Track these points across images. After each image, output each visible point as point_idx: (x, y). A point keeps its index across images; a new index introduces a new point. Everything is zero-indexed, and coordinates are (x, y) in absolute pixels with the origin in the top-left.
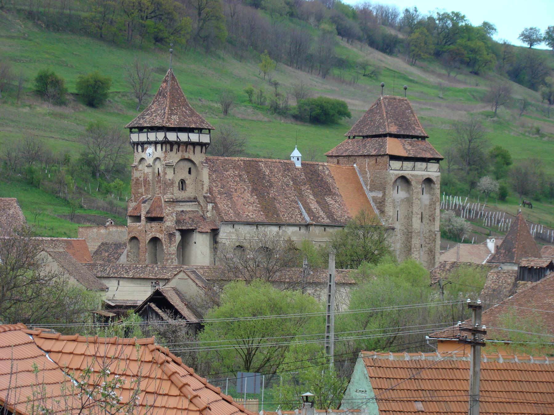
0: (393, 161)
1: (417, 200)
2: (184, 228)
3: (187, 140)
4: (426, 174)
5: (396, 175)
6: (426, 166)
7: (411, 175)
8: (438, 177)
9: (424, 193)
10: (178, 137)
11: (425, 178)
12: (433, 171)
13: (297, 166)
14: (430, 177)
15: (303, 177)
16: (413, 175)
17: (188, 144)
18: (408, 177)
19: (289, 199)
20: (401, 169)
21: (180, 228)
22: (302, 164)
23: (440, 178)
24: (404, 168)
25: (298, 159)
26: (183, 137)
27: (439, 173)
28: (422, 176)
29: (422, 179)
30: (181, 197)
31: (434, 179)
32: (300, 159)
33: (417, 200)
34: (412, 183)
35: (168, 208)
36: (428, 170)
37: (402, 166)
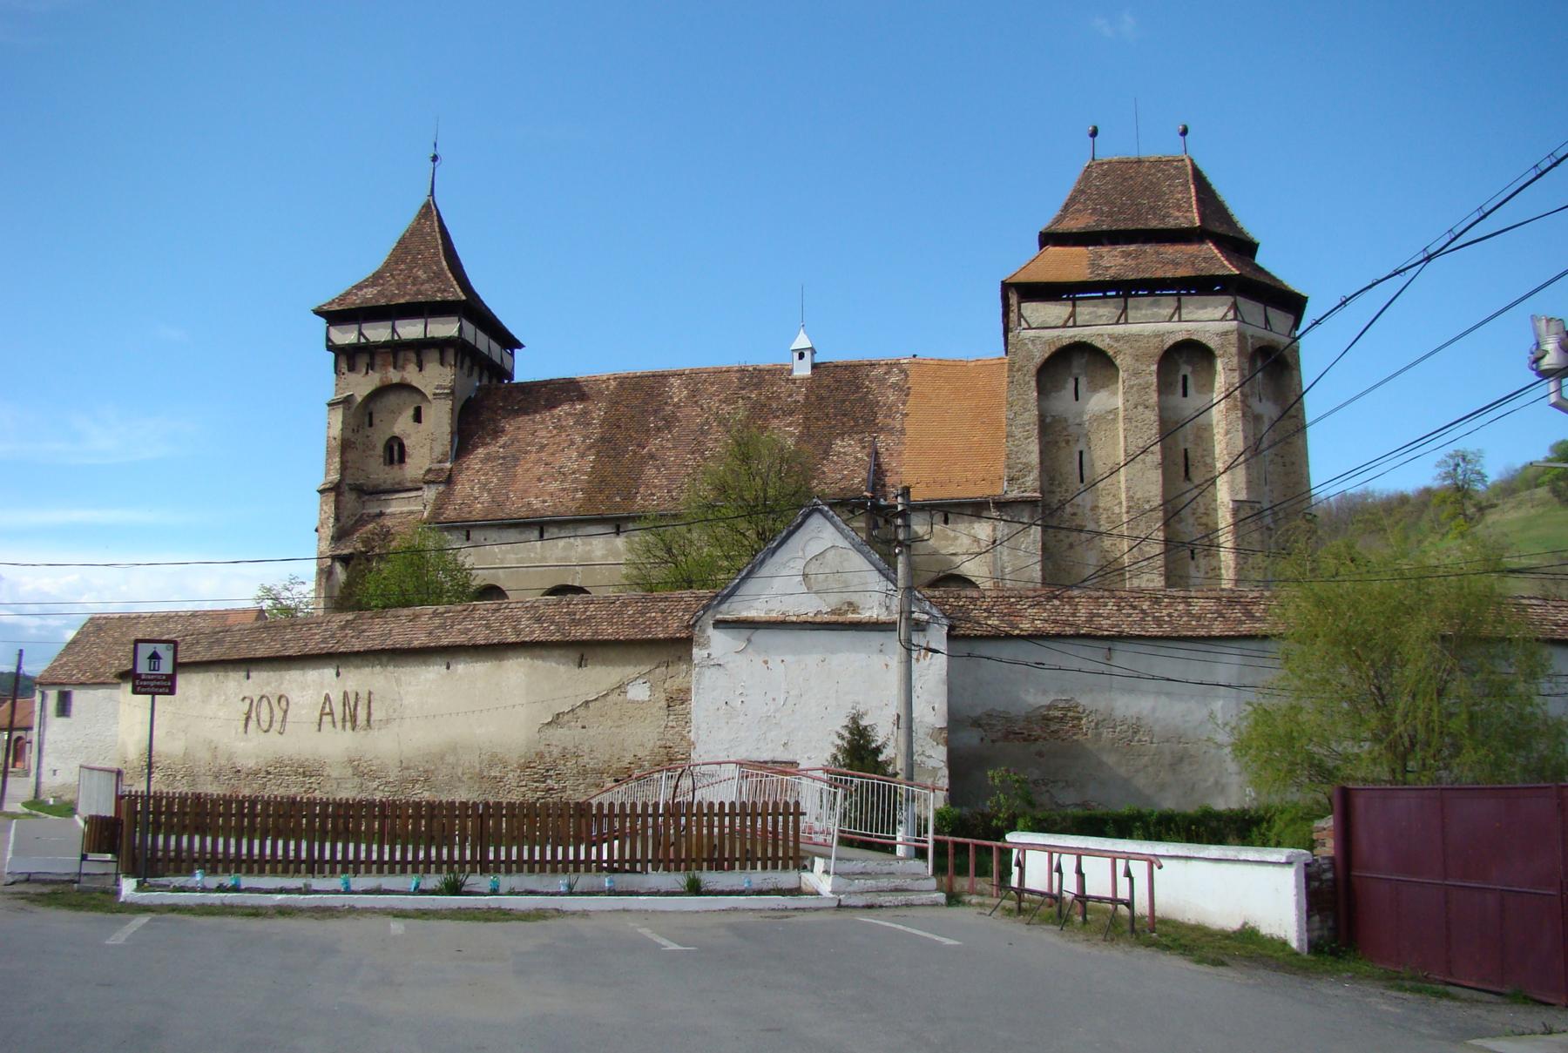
0: (1034, 304)
1: (1140, 408)
2: (346, 552)
3: (389, 338)
4: (1178, 330)
5: (1048, 343)
6: (1176, 304)
7: (1110, 336)
8: (1226, 333)
9: (1191, 390)
10: (361, 334)
11: (1171, 342)
12: (1205, 317)
13: (797, 374)
14: (1195, 338)
15: (801, 398)
16: (1116, 338)
17: (397, 349)
18: (1098, 344)
19: (703, 453)
20: (1071, 321)
21: (338, 552)
22: (815, 366)
23: (1234, 338)
24: (1079, 321)
25: (801, 356)
26: (378, 333)
27: (1236, 322)
28: (1157, 336)
29: (1156, 348)
30: (389, 482)
31: (1213, 344)
32: (807, 354)
33: (1140, 408)
34: (1118, 362)
35: (325, 507)
36: (1184, 317)
37: (1073, 315)
